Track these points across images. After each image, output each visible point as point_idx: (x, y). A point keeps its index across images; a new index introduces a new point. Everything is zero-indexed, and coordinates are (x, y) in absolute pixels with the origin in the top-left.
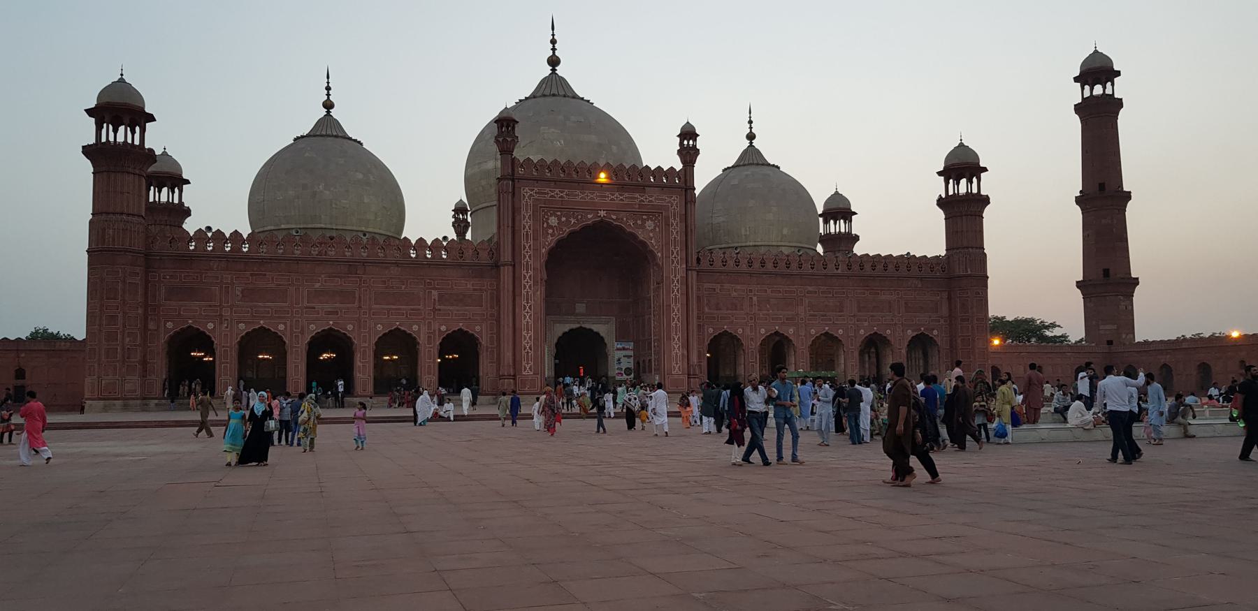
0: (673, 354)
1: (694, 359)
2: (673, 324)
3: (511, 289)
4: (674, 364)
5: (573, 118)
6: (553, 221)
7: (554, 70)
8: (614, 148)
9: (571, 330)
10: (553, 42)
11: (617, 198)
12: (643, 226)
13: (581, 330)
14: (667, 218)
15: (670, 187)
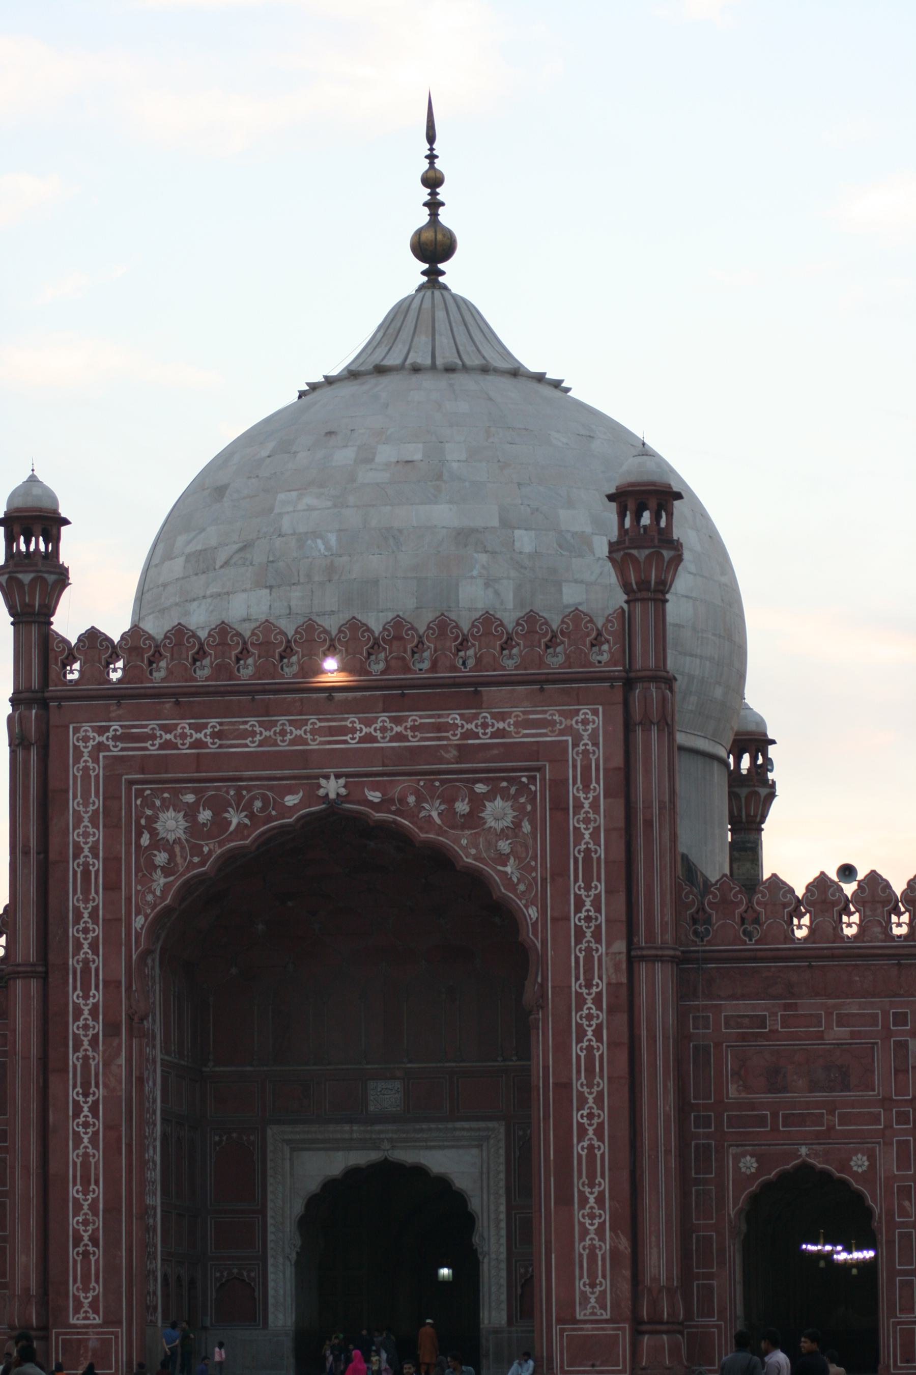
0: (580, 1248)
1: (659, 1262)
2: (579, 1149)
3: (34, 1051)
4: (581, 1285)
5: (386, 453)
6: (171, 824)
7: (433, 274)
8: (525, 541)
9: (353, 1173)
10: (433, 181)
11: (382, 730)
12: (473, 820)
13: (388, 1171)
14: (559, 786)
15: (571, 685)
